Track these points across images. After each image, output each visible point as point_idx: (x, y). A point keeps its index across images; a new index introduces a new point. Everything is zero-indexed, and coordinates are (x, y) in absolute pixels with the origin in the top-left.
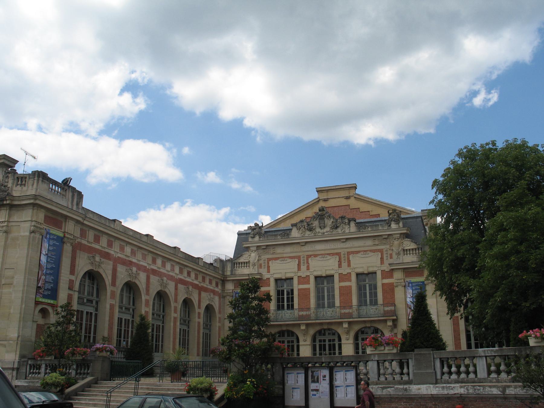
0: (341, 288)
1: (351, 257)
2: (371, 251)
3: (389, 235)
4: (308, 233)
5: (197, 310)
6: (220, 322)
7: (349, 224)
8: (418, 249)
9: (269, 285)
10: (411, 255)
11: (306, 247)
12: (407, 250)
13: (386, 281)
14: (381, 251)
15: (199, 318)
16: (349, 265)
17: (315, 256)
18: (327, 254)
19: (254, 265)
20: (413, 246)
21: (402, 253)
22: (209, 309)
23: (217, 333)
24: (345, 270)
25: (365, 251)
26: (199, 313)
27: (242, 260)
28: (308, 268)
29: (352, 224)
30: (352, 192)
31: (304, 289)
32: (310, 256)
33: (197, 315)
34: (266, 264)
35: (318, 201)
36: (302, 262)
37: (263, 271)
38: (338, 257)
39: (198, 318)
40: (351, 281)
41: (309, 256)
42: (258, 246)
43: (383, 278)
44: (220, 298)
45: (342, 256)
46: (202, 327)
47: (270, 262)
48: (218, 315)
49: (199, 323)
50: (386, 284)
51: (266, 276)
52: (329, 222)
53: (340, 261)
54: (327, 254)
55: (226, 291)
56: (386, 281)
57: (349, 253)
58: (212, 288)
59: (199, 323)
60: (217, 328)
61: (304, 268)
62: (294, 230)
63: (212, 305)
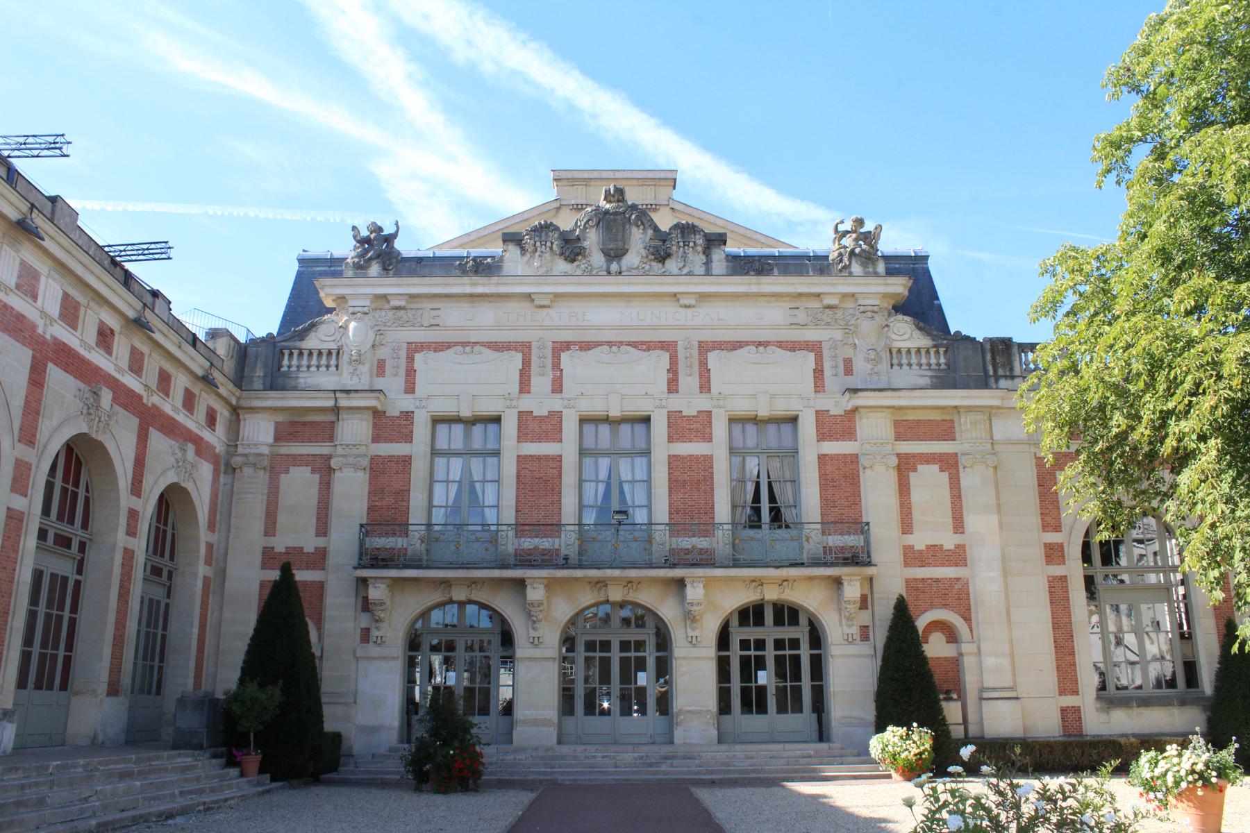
0: (673, 461)
1: (713, 358)
2: (780, 344)
3: (845, 296)
4: (562, 266)
5: (126, 500)
6: (208, 562)
7: (707, 251)
8: (937, 352)
9: (408, 438)
10: (905, 367)
11: (551, 311)
12: (899, 351)
13: (833, 448)
14: (815, 348)
15: (131, 532)
16: (705, 386)
17: (586, 346)
18: (629, 344)
19: (359, 360)
20: (923, 341)
21: (885, 355)
22: (172, 502)
23: (198, 602)
24: (690, 402)
25: (760, 344)
26: (133, 515)
27: (311, 342)
28: (557, 387)
29: (718, 255)
30: (663, 193)
31: (539, 458)
32: (567, 346)
33: (123, 521)
34: (403, 362)
35: (558, 209)
36: (535, 361)
37: (392, 383)
38: (666, 356)
39: (122, 538)
40: (710, 440)
41: (561, 348)
42: (377, 297)
43: (822, 437)
44: (216, 472)
45: (681, 353)
46: (139, 573)
47: (418, 357)
48: (204, 536)
49: (129, 554)
50: (832, 457)
51: (399, 402)
52: (638, 239)
53: (673, 371)
54: (629, 344)
55: (240, 450)
56: (833, 448)
57: (705, 348)
58: (191, 425)
59: (129, 554)
60: (200, 584)
61: (541, 382)
62: (513, 250)
63: (185, 492)
